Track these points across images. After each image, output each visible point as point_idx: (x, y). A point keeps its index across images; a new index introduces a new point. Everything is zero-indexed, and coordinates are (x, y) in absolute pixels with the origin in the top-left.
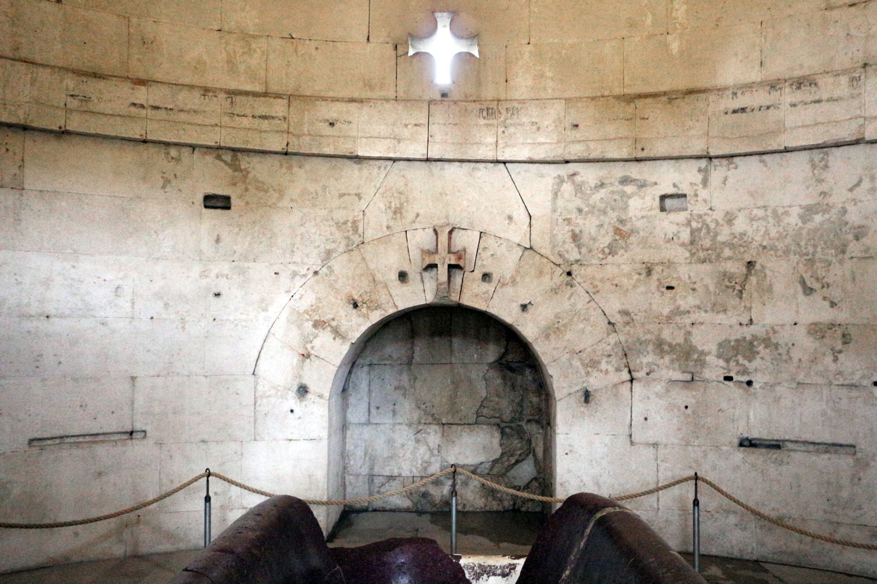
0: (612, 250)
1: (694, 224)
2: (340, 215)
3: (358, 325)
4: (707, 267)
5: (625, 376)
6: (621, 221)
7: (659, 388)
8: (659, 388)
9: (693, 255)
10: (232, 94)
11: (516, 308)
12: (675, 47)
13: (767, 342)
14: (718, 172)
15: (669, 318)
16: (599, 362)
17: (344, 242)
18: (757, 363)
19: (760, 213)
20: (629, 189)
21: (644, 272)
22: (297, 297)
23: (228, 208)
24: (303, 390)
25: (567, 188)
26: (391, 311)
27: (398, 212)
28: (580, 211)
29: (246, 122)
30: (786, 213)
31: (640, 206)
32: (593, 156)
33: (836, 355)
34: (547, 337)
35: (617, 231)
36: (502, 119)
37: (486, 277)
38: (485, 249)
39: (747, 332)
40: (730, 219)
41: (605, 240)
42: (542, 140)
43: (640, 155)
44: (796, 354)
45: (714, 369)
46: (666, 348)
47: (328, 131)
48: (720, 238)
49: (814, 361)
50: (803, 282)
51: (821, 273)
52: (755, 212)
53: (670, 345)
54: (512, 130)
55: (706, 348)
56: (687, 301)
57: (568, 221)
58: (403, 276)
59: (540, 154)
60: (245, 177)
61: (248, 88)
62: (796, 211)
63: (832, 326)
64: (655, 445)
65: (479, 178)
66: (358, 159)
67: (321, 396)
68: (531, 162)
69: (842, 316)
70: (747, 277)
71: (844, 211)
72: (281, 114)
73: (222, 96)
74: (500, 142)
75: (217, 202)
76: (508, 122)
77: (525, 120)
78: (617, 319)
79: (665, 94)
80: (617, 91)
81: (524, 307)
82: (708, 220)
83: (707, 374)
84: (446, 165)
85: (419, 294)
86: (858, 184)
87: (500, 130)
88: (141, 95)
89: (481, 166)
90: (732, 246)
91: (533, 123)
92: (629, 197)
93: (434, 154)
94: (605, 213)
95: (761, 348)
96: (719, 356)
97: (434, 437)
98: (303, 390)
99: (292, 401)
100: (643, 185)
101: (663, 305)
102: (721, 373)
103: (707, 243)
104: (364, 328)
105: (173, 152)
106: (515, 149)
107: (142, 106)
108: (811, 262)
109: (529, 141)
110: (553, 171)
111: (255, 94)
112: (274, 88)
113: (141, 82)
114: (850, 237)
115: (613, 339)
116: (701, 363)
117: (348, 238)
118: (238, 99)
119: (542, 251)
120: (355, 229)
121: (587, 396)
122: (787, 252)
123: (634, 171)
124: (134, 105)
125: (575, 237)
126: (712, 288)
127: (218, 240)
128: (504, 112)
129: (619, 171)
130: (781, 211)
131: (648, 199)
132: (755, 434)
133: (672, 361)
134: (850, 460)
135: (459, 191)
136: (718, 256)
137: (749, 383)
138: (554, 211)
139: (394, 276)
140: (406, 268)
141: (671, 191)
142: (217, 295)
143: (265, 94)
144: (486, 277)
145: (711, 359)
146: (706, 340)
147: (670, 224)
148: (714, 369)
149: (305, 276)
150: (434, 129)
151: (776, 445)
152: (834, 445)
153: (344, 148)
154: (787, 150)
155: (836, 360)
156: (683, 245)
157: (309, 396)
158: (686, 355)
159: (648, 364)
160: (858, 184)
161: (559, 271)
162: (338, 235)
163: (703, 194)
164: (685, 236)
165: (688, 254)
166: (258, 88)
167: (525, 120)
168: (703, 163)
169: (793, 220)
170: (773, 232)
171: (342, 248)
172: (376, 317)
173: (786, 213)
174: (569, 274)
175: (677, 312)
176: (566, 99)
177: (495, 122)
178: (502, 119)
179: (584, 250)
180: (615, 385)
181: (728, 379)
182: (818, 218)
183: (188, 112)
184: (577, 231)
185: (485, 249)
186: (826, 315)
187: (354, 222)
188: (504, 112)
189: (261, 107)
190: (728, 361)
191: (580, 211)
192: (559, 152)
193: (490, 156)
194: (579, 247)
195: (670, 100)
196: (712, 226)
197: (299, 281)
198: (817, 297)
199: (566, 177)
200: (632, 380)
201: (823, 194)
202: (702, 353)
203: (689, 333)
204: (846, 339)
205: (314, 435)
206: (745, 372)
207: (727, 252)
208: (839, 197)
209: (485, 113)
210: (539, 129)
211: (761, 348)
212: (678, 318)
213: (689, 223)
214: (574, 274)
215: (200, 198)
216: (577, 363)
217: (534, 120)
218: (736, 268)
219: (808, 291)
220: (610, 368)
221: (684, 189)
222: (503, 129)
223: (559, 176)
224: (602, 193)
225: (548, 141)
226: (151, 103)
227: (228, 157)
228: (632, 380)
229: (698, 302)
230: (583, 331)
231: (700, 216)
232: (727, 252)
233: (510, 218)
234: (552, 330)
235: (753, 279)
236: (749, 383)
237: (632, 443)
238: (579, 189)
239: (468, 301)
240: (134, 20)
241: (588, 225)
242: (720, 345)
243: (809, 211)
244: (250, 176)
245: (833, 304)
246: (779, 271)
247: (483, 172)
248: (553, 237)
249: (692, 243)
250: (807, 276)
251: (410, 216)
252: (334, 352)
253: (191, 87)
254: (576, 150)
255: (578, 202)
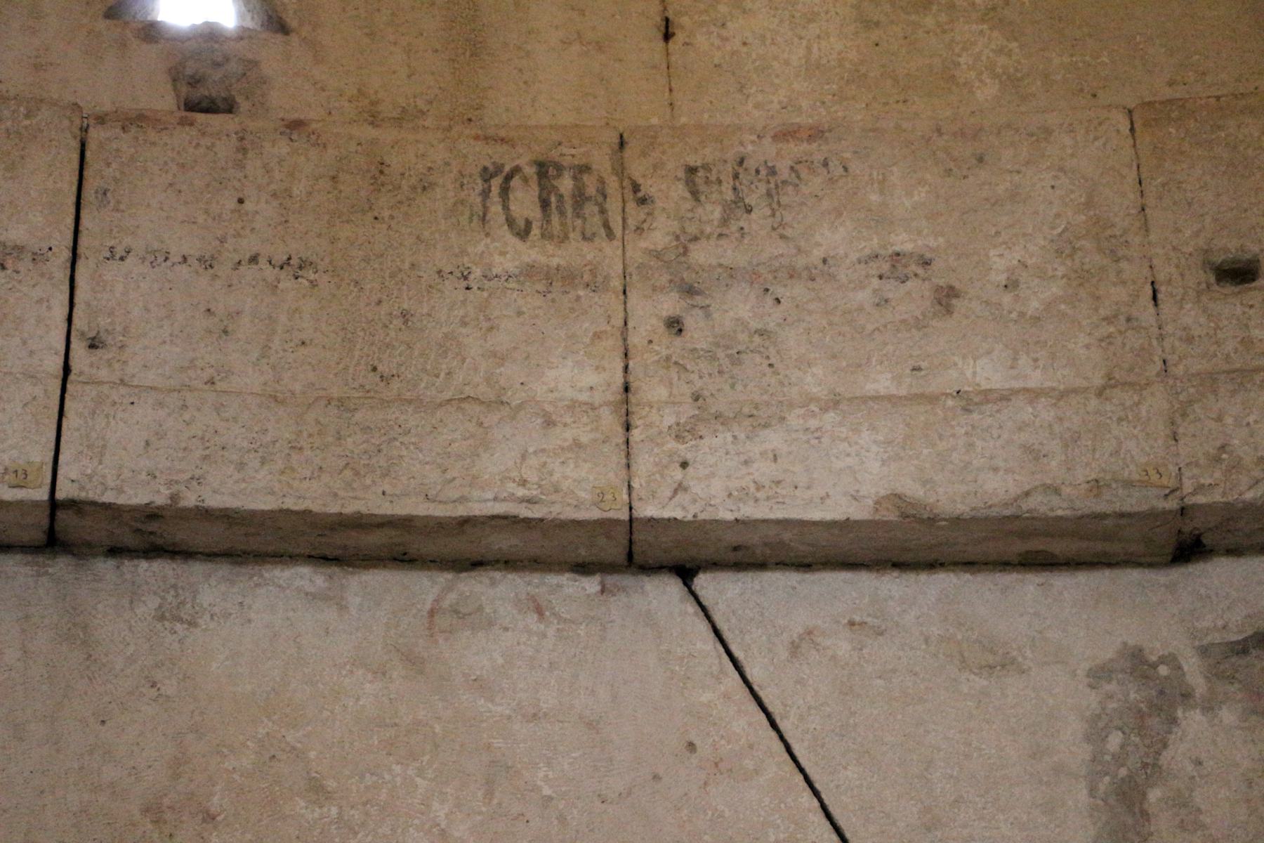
36: (660, 236)
42: (987, 372)
54: (738, 308)
59: (980, 474)
65: (480, 685)
74: (651, 390)
76: (701, 254)
87: (648, 312)
91: (897, 265)
93: (119, 462)
106: (773, 439)
109: (882, 383)
110: (1075, 622)
128: (669, 193)
135: (317, 790)
150: (113, 291)
167: (834, 239)
177: (609, 256)
178: (660, 236)
188: (669, 193)
193: (576, 483)
199: (1194, 672)
209: (524, 201)
210: (946, 298)
217: (903, 242)
222: (670, 304)
223: (1137, 663)
225: (1035, 379)
247: (519, 636)
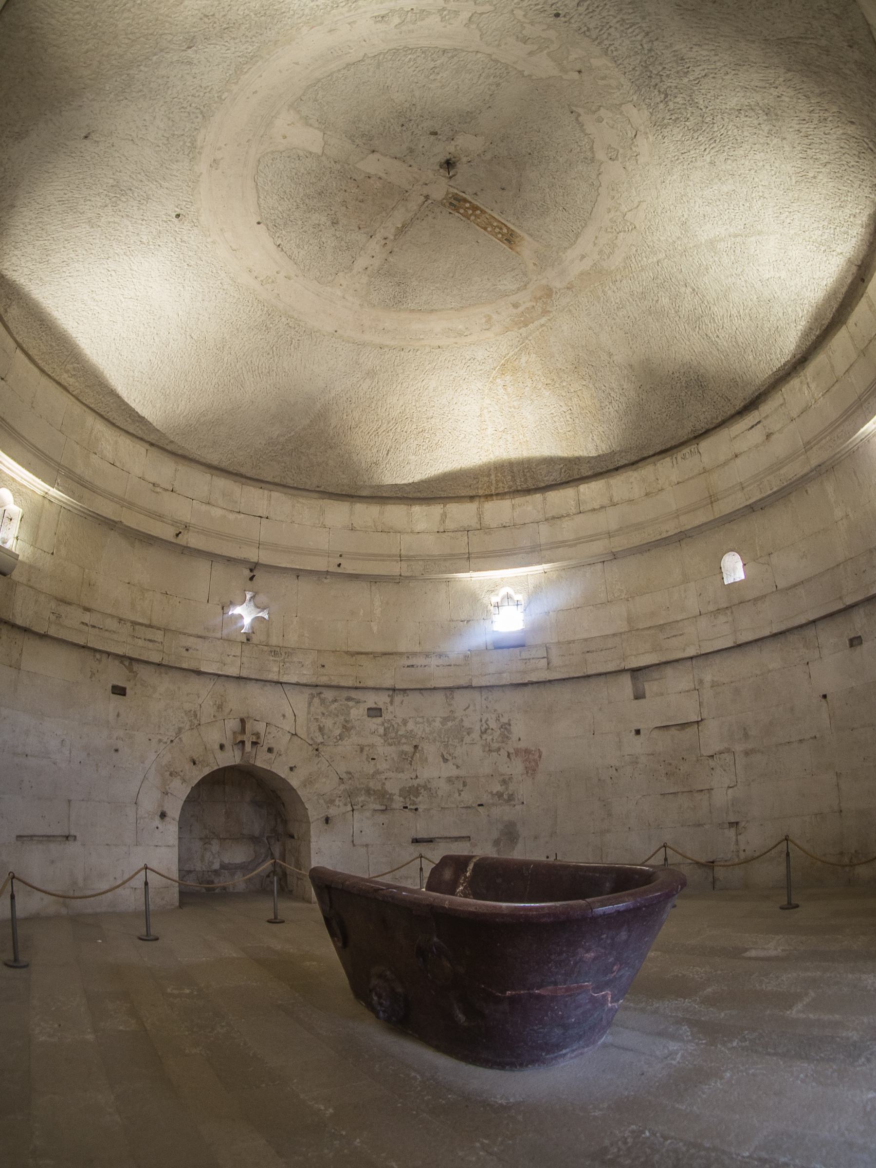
0: (341, 737)
1: (386, 725)
2: (187, 706)
3: (197, 775)
4: (393, 747)
5: (349, 808)
6: (346, 721)
7: (368, 814)
8: (368, 814)
9: (385, 741)
10: (134, 623)
11: (287, 768)
12: (375, 629)
13: (425, 787)
14: (398, 698)
15: (373, 776)
16: (334, 801)
17: (189, 723)
18: (420, 798)
19: (420, 720)
20: (351, 704)
21: (359, 750)
22: (161, 755)
23: (124, 695)
24: (163, 815)
25: (316, 700)
26: (216, 768)
27: (220, 707)
28: (323, 714)
29: (140, 643)
30: (434, 721)
31: (357, 713)
32: (333, 684)
33: (460, 792)
34: (305, 786)
35: (344, 727)
37: (270, 750)
38: (269, 733)
39: (415, 783)
40: (405, 722)
41: (337, 732)
43: (358, 685)
44: (440, 793)
45: (398, 802)
46: (372, 792)
47: (185, 653)
48: (399, 733)
49: (449, 796)
50: (443, 756)
51: (452, 751)
52: (418, 719)
53: (374, 791)
54: (288, 664)
55: (393, 792)
56: (382, 765)
57: (317, 720)
58: (222, 747)
59: (304, 680)
60: (135, 676)
61: (141, 621)
62: (438, 720)
63: (457, 777)
64: (367, 846)
66: (199, 673)
67: (174, 819)
68: (297, 684)
69: (462, 772)
70: (414, 753)
71: (462, 720)
72: (159, 640)
73: (129, 624)
75: (119, 691)
77: (295, 659)
78: (344, 776)
79: (371, 653)
80: (344, 648)
81: (291, 769)
82: (394, 723)
83: (394, 806)
84: (248, 682)
85: (231, 758)
86: (467, 708)
87: (282, 664)
88: (87, 617)
89: (268, 684)
90: (406, 737)
91: (300, 662)
92: (352, 707)
93: (244, 674)
94: (337, 716)
95: (422, 791)
96: (400, 796)
97: (215, 847)
98: (163, 815)
99: (157, 822)
100: (358, 702)
101: (369, 768)
102: (401, 805)
103: (393, 735)
104: (200, 778)
105: (98, 656)
107: (87, 625)
108: (446, 746)
110: (308, 691)
111: (146, 626)
112: (154, 623)
113: (87, 609)
114: (465, 733)
115: (342, 787)
116: (391, 799)
117: (191, 721)
118: (137, 627)
119: (302, 736)
120: (196, 716)
121: (327, 820)
122: (434, 741)
123: (353, 694)
124: (83, 623)
125: (321, 729)
126: (396, 759)
127: (118, 715)
129: (346, 694)
130: (431, 719)
131: (361, 710)
132: (420, 836)
133: (375, 799)
134: (468, 844)
136: (399, 742)
137: (416, 809)
138: (309, 713)
139: (217, 747)
140: (224, 742)
141: (374, 706)
142: (116, 750)
143: (150, 626)
144: (270, 750)
145: (396, 798)
146: (392, 788)
147: (374, 723)
148: (398, 802)
149: (166, 743)
151: (430, 841)
152: (460, 837)
153: (193, 665)
154: (435, 689)
155: (460, 795)
156: (380, 736)
157: (167, 819)
158: (383, 796)
159: (362, 801)
160: (467, 708)
161: (310, 748)
162: (186, 719)
163: (390, 708)
164: (381, 731)
165: (382, 741)
166: (146, 621)
168: (391, 693)
169: (437, 724)
170: (427, 730)
171: (187, 727)
172: (207, 771)
173: (434, 721)
174: (317, 750)
175: (377, 772)
176: (319, 651)
179: (325, 737)
180: (344, 814)
181: (406, 807)
182: (450, 724)
183: (110, 631)
184: (322, 725)
185: (269, 733)
186: (455, 772)
187: (195, 712)
189: (150, 634)
190: (405, 798)
191: (323, 714)
192: (313, 680)
194: (323, 735)
195: (375, 657)
196: (396, 726)
197: (162, 746)
198: (450, 764)
200: (353, 810)
201: (451, 711)
202: (391, 794)
203: (384, 784)
204: (465, 784)
205: (170, 843)
206: (414, 803)
207: (404, 740)
208: (459, 714)
211: (422, 791)
212: (378, 776)
213: (383, 724)
214: (320, 750)
215: (109, 687)
216: (322, 801)
218: (409, 749)
219: (445, 760)
220: (341, 804)
221: (381, 705)
224: (336, 705)
226: (91, 623)
227: (127, 663)
228: (353, 810)
229: (388, 767)
230: (325, 783)
231: (389, 721)
232: (404, 740)
233: (284, 716)
234: (308, 782)
235: (418, 755)
236: (416, 809)
237: (354, 845)
238: (323, 701)
239: (259, 763)
240: (87, 570)
241: (328, 723)
242: (401, 790)
243: (445, 720)
244: (138, 676)
245: (458, 767)
246: (431, 750)
247: (269, 689)
248: (308, 728)
249: (385, 735)
250: (444, 753)
251: (227, 710)
252: (181, 790)
253: (112, 616)
254: (324, 680)
255: (322, 709)
